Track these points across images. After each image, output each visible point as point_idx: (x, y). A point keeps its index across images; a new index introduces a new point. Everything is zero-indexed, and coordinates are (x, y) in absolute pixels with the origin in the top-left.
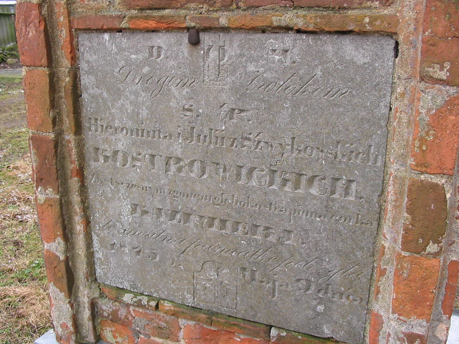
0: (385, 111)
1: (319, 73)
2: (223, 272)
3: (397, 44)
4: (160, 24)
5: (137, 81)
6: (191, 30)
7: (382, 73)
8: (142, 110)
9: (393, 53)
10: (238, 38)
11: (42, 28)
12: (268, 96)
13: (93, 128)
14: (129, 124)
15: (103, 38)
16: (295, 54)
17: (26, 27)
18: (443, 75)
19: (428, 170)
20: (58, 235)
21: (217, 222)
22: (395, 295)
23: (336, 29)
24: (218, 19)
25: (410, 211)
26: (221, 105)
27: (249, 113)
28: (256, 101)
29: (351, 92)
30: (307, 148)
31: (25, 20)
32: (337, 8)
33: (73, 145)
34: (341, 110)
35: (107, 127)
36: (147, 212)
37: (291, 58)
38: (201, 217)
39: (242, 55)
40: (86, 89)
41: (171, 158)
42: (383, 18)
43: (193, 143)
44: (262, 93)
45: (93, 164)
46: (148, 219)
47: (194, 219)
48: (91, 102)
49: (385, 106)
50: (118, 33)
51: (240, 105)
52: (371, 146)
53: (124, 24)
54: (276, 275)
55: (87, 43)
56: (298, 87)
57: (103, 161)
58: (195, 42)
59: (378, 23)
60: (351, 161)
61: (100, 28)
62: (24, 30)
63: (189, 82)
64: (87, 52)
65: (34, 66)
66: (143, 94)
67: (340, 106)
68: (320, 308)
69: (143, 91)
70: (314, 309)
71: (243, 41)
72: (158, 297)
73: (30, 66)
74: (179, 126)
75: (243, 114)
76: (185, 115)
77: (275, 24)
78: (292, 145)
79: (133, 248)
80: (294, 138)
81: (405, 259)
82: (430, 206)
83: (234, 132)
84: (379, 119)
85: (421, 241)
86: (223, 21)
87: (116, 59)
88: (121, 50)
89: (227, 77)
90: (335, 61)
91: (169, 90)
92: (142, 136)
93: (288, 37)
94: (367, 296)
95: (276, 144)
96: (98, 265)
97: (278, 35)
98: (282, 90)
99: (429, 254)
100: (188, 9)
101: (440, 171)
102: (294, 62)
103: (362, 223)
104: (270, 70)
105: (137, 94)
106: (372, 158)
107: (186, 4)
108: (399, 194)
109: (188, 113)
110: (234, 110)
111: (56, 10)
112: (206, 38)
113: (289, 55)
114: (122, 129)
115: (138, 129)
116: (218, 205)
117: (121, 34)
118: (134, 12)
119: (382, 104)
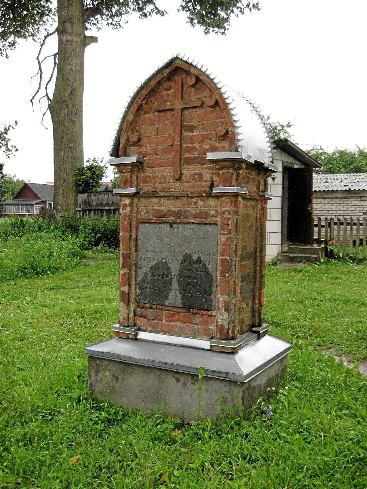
10: (183, 225)
14: (152, 249)
18: (225, 233)
33: (135, 256)
45: (140, 262)
53: (152, 221)
58: (171, 226)
86: (178, 221)
105: (154, 240)
112: (174, 226)
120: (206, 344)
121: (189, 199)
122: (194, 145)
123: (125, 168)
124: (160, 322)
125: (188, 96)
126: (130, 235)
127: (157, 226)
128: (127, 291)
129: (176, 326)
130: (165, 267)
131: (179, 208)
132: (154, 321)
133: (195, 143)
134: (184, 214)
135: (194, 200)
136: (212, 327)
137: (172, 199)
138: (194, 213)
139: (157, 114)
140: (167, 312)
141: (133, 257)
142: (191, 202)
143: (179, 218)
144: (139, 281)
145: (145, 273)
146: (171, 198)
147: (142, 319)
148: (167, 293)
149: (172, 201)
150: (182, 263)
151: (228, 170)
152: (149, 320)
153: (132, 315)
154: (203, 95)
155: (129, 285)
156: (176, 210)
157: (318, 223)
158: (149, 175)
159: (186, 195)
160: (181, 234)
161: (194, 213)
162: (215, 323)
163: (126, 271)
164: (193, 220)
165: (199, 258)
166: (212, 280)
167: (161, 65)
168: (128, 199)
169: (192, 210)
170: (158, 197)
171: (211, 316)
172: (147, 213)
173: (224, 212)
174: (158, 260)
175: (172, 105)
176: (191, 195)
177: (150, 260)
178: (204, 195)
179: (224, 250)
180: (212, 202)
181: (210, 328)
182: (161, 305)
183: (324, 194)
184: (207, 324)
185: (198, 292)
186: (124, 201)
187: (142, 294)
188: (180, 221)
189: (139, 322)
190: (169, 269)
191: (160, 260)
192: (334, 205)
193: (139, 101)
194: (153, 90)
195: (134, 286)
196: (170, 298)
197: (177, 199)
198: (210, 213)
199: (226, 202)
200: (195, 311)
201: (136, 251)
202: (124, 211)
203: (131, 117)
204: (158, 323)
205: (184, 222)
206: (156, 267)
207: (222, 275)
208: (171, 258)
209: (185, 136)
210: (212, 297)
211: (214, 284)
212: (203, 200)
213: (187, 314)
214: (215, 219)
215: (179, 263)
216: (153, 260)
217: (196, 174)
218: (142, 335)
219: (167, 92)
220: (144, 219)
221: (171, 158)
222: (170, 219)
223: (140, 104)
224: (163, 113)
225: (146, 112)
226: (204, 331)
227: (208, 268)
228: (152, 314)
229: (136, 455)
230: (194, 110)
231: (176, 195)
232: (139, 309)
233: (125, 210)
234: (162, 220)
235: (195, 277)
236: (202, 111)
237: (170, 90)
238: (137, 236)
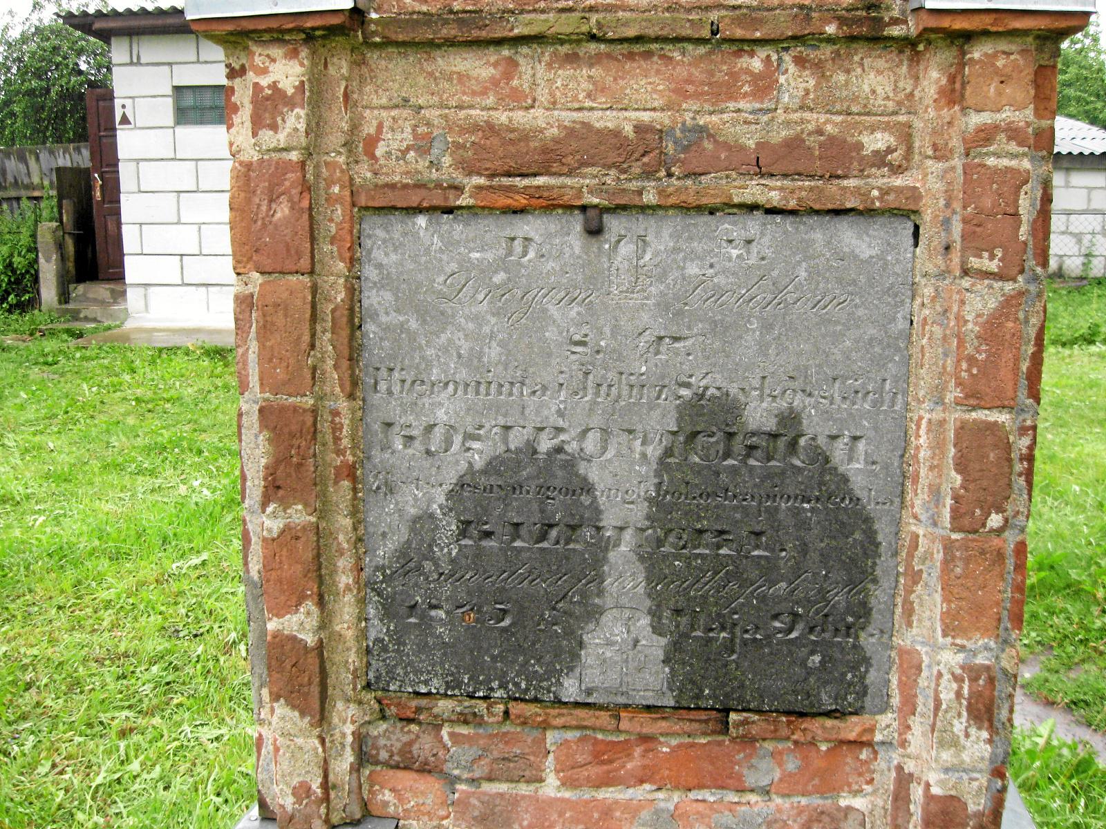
0: (902, 324)
1: (803, 274)
2: (638, 624)
3: (917, 228)
4: (534, 200)
5: (480, 297)
6: (589, 210)
7: (898, 269)
8: (490, 348)
9: (911, 241)
11: (305, 204)
12: (722, 314)
13: (383, 386)
14: (463, 374)
15: (414, 224)
17: (271, 201)
18: (993, 266)
19: (983, 403)
22: (944, 605)
23: (830, 206)
25: (961, 467)
26: (641, 331)
27: (689, 343)
28: (701, 321)
29: (852, 300)
30: (785, 391)
31: (271, 190)
32: (827, 176)
34: (839, 328)
35: (414, 382)
37: (758, 253)
39: (676, 250)
40: (374, 316)
41: (542, 429)
42: (899, 190)
43: (586, 399)
44: (711, 309)
45: (377, 456)
48: (381, 339)
49: (904, 318)
50: (445, 216)
51: (674, 330)
52: (884, 380)
53: (465, 200)
54: (736, 613)
55: (380, 233)
56: (770, 297)
57: (401, 447)
58: (595, 231)
59: (891, 197)
60: (856, 407)
61: (415, 205)
62: (264, 208)
63: (583, 296)
64: (379, 248)
65: (280, 273)
66: (493, 320)
67: (837, 323)
69: (493, 315)
70: (803, 663)
71: (679, 228)
72: (505, 696)
73: (270, 273)
74: (562, 372)
75: (677, 345)
76: (574, 353)
77: (736, 200)
78: (761, 389)
79: (458, 607)
80: (764, 378)
81: (957, 544)
82: (988, 457)
83: (663, 377)
84: (897, 339)
85: (978, 512)
86: (650, 198)
87: (441, 260)
88: (450, 244)
89: (651, 285)
90: (828, 255)
91: (545, 311)
92: (488, 394)
93: (753, 220)
94: (890, 624)
96: (375, 653)
97: (736, 218)
98: (744, 302)
99: (992, 531)
100: (584, 177)
101: (999, 403)
102: (763, 259)
103: (878, 503)
104: (724, 272)
106: (887, 398)
107: (579, 168)
108: (938, 446)
109: (579, 349)
110: (661, 338)
112: (614, 225)
113: (754, 248)
114: (447, 384)
115: (479, 383)
116: (632, 503)
117: (451, 216)
118: (482, 181)
119: (899, 315)
121: (717, 57)
124: (524, 789)
126: (314, 289)
127: (493, 230)
128: (310, 639)
129: (632, 810)
130: (558, 483)
131: (646, 117)
132: (487, 787)
134: (686, 149)
135: (756, 64)
136: (859, 803)
138: (751, 144)
140: (571, 735)
141: (336, 428)
142: (733, 75)
143: (648, 174)
144: (381, 568)
145: (416, 520)
146: (593, 47)
147: (405, 779)
148: (569, 633)
149: (596, 72)
150: (668, 452)
152: (452, 781)
153: (343, 764)
155: (321, 602)
156: (628, 129)
159: (706, 33)
160: (662, 278)
161: (751, 144)
163: (299, 515)
164: (753, 191)
165: (790, 419)
166: (871, 544)
168: (294, 54)
170: (499, 42)
171: (858, 744)
172: (423, 145)
173: (986, 135)
174: (505, 441)
176: (739, 33)
177: (448, 443)
178: (831, 29)
179: (984, 371)
181: (849, 809)
182: (536, 700)
184: (829, 787)
185: (776, 617)
186: (264, 71)
187: (400, 643)
188: (661, 192)
189: (388, 796)
190: (588, 488)
191: (517, 439)
195: (349, 598)
196: (588, 657)
197: (631, 56)
198: (859, 146)
199: (997, 71)
200: (758, 723)
201: (353, 388)
202: (267, 136)
204: (515, 801)
205: (692, 200)
206: (493, 480)
207: (966, 521)
208: (596, 421)
210: (868, 640)
211: (884, 562)
212: (818, 66)
213: (703, 741)
214: (898, 182)
215: (655, 451)
216: (468, 437)
220: (406, 186)
227: (845, 480)
228: (473, 752)
231: (631, 32)
232: (383, 726)
233: (274, 127)
235: (758, 534)
238: (354, 293)
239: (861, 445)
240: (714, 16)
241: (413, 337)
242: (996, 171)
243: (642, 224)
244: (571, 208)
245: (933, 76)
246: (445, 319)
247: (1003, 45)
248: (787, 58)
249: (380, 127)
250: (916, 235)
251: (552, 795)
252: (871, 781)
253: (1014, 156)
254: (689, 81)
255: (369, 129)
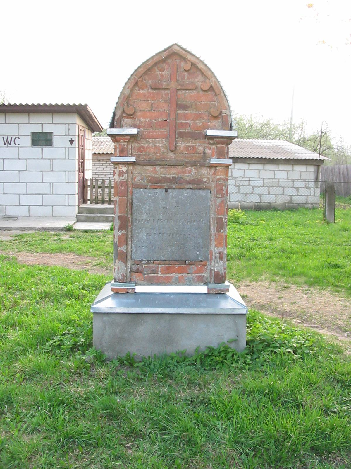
0: (209, 204)
1: (195, 198)
10: (177, 190)
16: (190, 194)
18: (220, 196)
20: (124, 244)
21: (171, 235)
24: (173, 186)
36: (151, 235)
38: (167, 234)
45: (135, 224)
46: (151, 237)
47: (165, 235)
53: (148, 187)
55: (136, 191)
58: (166, 191)
68: (198, 253)
86: (174, 187)
88: (146, 193)
91: (159, 203)
95: (186, 214)
111: (129, 183)
112: (169, 190)
120: (203, 289)
122: (187, 122)
123: (123, 138)
124: (155, 275)
125: (182, 79)
127: (151, 191)
129: (172, 277)
131: (173, 176)
132: (149, 275)
133: (188, 120)
137: (167, 168)
138: (188, 180)
139: (151, 91)
143: (174, 184)
151: (222, 146)
154: (196, 80)
156: (171, 177)
157: (102, 184)
158: (144, 145)
161: (188, 180)
162: (209, 270)
163: (124, 231)
164: (188, 186)
167: (162, 49)
168: (126, 166)
169: (187, 177)
172: (142, 179)
173: (219, 179)
175: (168, 85)
180: (205, 171)
183: (99, 156)
192: (108, 167)
193: (136, 77)
194: (149, 70)
198: (203, 180)
203: (127, 92)
209: (178, 113)
214: (208, 185)
217: (190, 146)
218: (139, 289)
219: (161, 73)
221: (165, 132)
222: (165, 185)
223: (137, 81)
224: (157, 91)
225: (141, 88)
226: (198, 279)
229: (60, 411)
230: (187, 92)
233: (122, 176)
234: (159, 186)
236: (195, 93)
237: (164, 71)
239: (204, 221)
240: (183, 162)
241: (140, 206)
242: (220, 184)
243: (173, 190)
244: (163, 188)
245: (213, 171)
246: (145, 204)
247: (221, 168)
248: (193, 168)
249: (136, 176)
250: (210, 192)
251: (160, 276)
252: (207, 271)
253: (223, 182)
254: (180, 171)
255: (135, 176)
